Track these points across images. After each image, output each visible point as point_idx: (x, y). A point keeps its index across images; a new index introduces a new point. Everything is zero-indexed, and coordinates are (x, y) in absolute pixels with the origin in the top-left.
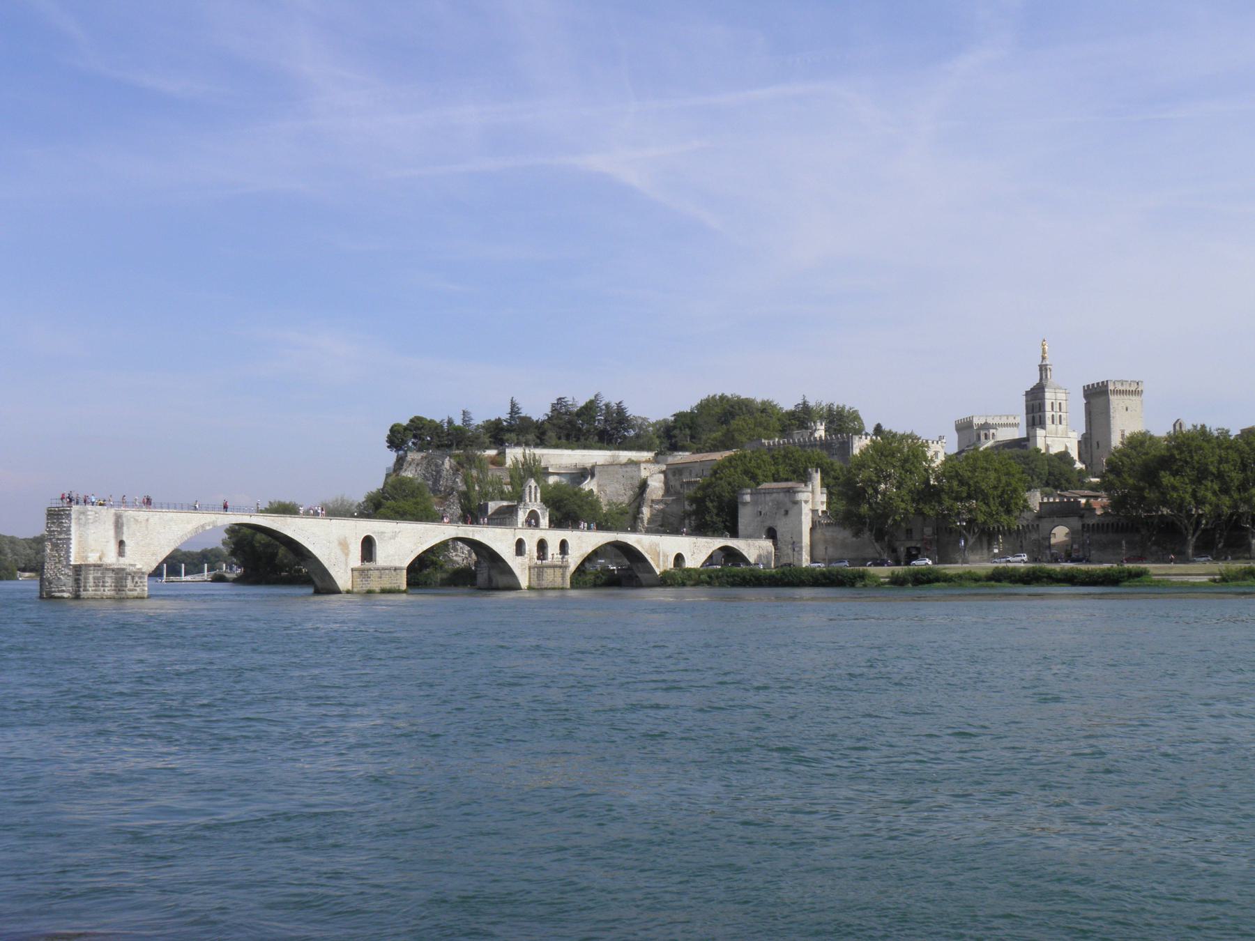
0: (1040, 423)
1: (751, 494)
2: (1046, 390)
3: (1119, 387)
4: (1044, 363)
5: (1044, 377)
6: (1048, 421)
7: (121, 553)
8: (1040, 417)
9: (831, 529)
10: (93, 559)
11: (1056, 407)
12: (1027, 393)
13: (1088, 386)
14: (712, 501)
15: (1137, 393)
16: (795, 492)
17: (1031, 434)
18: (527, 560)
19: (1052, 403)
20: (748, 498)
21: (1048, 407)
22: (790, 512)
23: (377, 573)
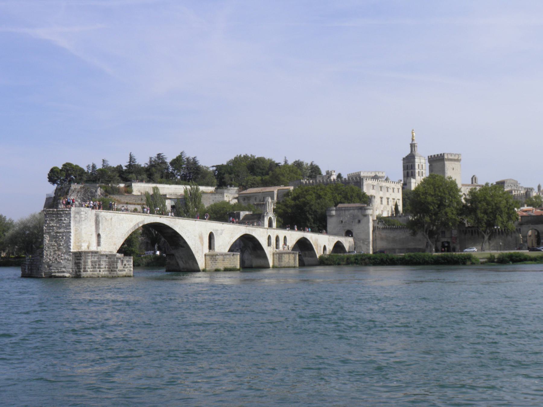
0: (412, 175)
1: (336, 210)
2: (416, 157)
3: (450, 157)
4: (413, 143)
5: (413, 150)
6: (417, 175)
7: (99, 244)
8: (412, 172)
9: (385, 231)
10: (84, 248)
11: (420, 167)
12: (404, 159)
13: (431, 156)
14: (311, 214)
15: (458, 160)
16: (366, 209)
17: (408, 181)
18: (272, 249)
19: (419, 165)
20: (334, 213)
21: (417, 167)
22: (361, 221)
23: (221, 257)
